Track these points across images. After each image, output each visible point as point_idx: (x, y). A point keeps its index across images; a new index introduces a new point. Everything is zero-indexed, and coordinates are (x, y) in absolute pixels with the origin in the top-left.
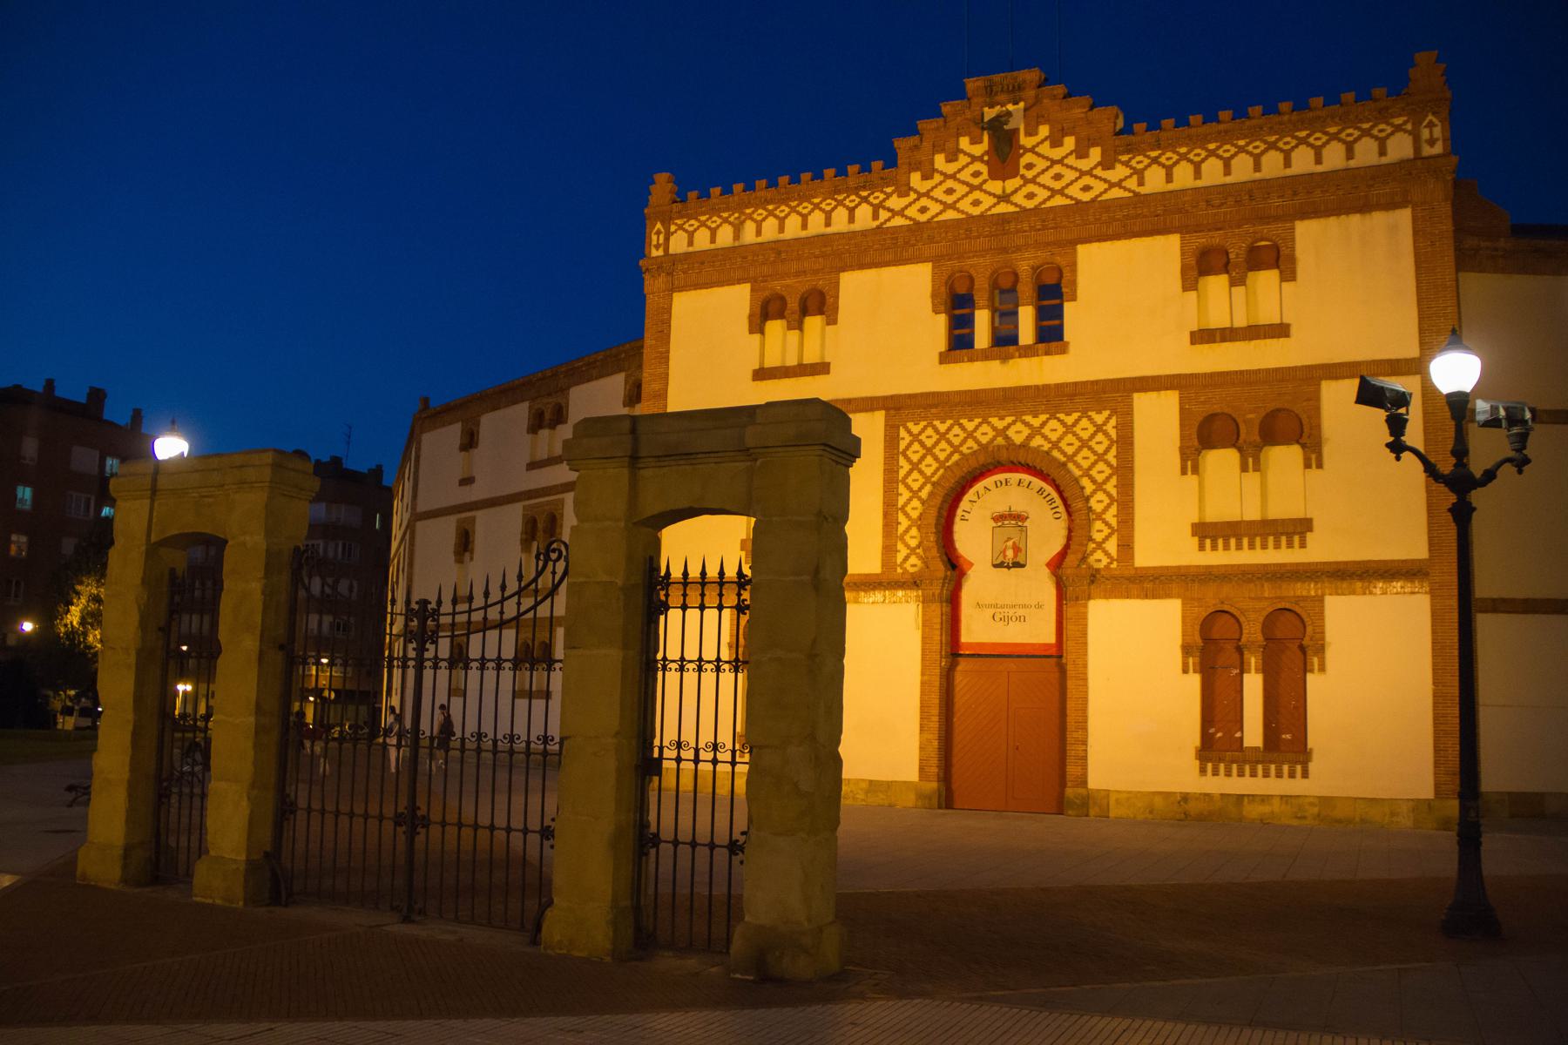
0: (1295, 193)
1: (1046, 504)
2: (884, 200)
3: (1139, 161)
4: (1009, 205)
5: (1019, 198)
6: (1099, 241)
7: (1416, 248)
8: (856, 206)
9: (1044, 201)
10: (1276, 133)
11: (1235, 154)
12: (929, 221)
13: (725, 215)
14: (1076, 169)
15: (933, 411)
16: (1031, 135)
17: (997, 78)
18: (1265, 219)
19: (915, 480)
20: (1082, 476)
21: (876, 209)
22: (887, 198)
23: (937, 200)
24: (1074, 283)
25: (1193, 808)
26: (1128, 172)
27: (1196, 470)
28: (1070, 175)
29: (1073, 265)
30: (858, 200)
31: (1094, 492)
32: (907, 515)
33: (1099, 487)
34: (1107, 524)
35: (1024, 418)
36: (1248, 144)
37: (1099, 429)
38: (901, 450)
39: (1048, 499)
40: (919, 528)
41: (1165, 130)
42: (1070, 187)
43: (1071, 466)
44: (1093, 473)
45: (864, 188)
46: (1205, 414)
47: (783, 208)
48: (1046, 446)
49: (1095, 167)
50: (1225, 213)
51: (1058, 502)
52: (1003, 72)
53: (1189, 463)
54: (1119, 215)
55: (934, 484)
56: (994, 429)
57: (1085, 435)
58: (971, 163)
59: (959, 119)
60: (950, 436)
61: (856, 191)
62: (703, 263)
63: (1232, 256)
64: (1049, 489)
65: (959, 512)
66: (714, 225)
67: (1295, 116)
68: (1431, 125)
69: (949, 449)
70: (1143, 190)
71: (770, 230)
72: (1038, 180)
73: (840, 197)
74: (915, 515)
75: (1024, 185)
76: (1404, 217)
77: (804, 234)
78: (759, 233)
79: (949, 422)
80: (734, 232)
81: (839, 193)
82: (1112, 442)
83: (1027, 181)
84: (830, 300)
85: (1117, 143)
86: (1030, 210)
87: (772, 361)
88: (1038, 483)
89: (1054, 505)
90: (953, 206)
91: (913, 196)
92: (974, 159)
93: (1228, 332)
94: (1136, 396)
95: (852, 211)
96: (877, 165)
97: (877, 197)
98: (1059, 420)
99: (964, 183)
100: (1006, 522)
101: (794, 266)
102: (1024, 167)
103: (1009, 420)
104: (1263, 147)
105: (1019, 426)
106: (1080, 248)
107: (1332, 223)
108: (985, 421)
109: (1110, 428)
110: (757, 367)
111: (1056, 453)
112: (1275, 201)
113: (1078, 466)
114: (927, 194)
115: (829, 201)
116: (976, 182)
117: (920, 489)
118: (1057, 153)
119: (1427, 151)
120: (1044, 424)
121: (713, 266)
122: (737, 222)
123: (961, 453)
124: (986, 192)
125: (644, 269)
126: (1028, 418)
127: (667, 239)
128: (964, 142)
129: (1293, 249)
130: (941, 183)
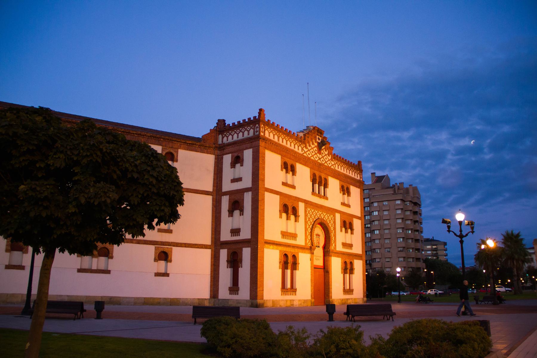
15: (312, 206)
21: (302, 149)
25: (343, 301)
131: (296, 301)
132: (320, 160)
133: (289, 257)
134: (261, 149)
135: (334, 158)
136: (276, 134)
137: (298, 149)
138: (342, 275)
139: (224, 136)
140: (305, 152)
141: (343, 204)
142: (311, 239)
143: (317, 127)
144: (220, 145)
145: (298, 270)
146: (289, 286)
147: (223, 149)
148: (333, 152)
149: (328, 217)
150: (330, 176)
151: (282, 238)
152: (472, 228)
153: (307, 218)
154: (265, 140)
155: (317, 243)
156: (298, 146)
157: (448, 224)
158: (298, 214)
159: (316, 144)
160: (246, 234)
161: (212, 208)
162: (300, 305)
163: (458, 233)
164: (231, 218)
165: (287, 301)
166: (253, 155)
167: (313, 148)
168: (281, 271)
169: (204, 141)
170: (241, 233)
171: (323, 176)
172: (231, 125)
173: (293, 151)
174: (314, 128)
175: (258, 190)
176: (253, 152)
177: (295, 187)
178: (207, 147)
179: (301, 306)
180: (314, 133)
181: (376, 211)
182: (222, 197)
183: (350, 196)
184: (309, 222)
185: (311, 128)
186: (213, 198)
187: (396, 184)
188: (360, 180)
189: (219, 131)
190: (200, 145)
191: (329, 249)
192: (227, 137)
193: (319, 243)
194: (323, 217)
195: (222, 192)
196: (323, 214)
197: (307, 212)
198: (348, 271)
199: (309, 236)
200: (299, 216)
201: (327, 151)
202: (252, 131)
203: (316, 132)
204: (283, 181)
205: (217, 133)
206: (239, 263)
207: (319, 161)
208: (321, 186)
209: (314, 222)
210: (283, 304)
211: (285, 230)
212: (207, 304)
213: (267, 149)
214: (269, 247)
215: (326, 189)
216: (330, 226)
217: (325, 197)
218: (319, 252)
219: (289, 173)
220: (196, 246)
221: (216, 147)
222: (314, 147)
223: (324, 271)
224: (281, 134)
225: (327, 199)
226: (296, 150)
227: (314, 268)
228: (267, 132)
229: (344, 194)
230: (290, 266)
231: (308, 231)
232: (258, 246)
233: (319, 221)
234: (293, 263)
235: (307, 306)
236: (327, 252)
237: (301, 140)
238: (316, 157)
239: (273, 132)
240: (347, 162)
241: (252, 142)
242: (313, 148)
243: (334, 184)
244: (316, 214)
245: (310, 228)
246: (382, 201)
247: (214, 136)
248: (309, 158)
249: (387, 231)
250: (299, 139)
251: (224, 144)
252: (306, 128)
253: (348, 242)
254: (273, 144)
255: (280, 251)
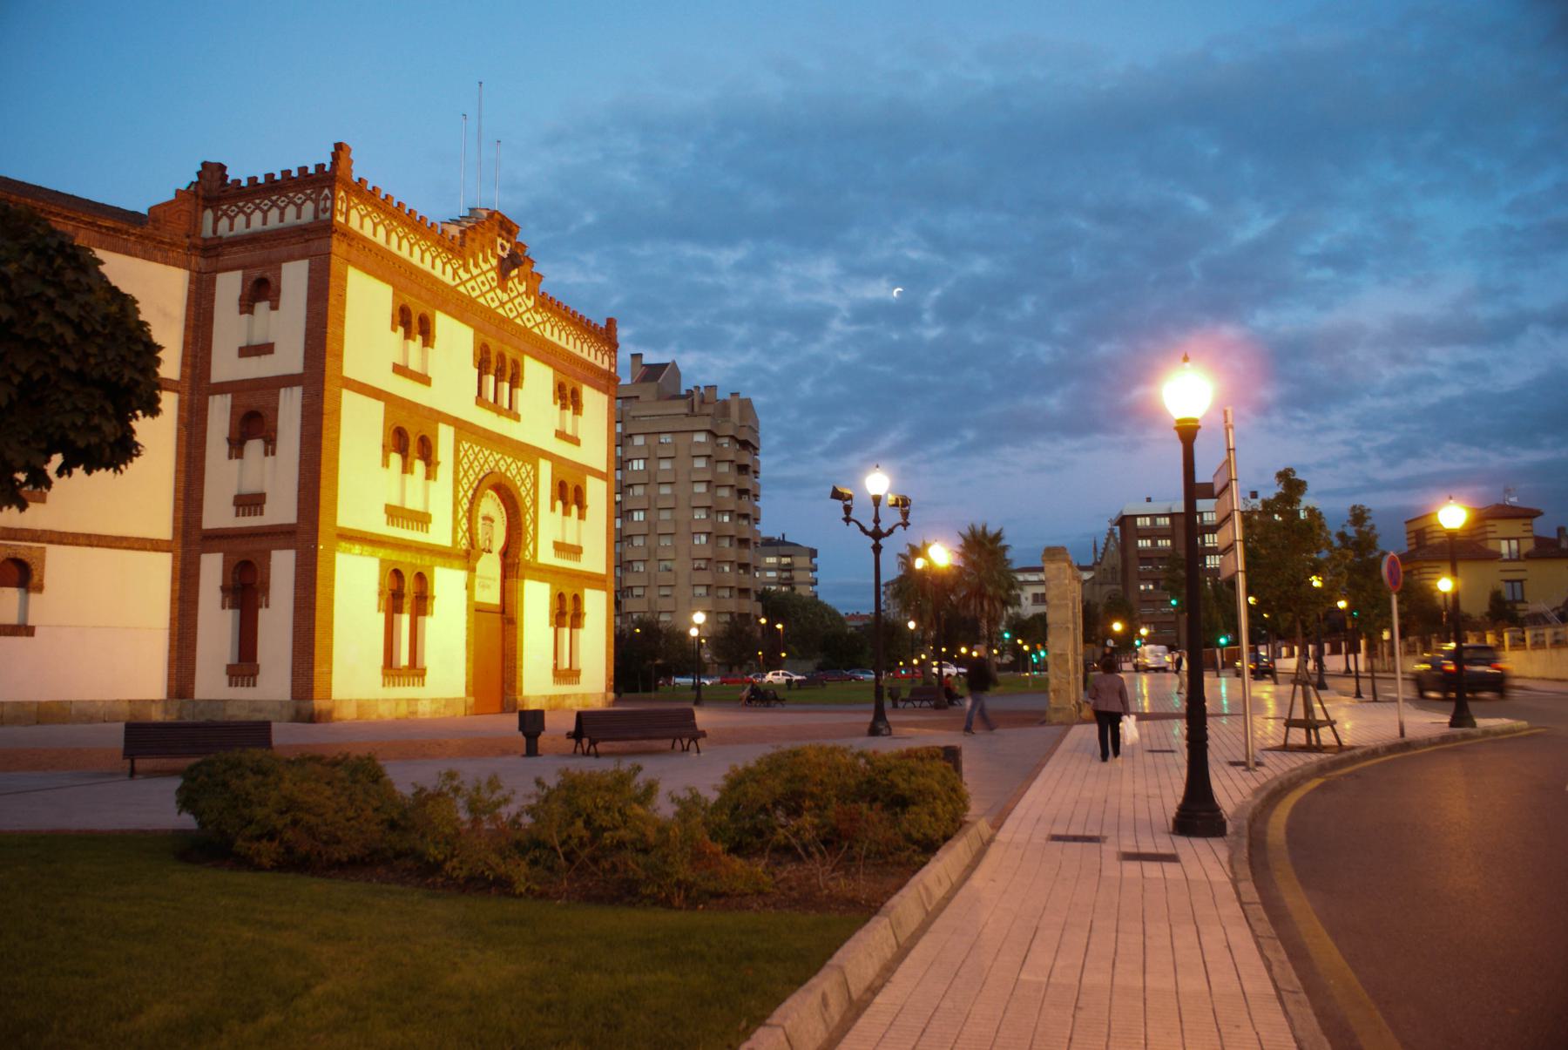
15: (474, 436)
21: (455, 273)
131: (424, 702)
132: (504, 308)
133: (406, 579)
134: (335, 262)
135: (543, 305)
136: (381, 222)
137: (442, 270)
138: (552, 630)
139: (222, 216)
140: (463, 283)
141: (561, 435)
142: (470, 529)
143: (499, 214)
144: (205, 240)
145: (432, 614)
146: (404, 660)
147: (218, 255)
148: (542, 288)
149: (519, 469)
150: (528, 354)
151: (388, 524)
152: (905, 515)
153: (461, 469)
154: (349, 236)
155: (485, 541)
156: (444, 264)
157: (846, 500)
158: (436, 457)
159: (494, 262)
160: (281, 510)
161: (179, 430)
162: (435, 712)
163: (870, 527)
164: (236, 462)
165: (397, 702)
166: (310, 278)
167: (484, 273)
168: (382, 616)
169: (157, 225)
170: (266, 507)
171: (509, 354)
172: (244, 183)
173: (427, 275)
174: (492, 214)
175: (323, 382)
176: (311, 270)
177: (430, 379)
178: (163, 243)
179: (437, 716)
180: (490, 230)
181: (638, 459)
182: (211, 398)
183: (581, 415)
184: (465, 480)
185: (482, 215)
186: (181, 402)
187: (697, 388)
188: (609, 371)
189: (204, 199)
190: (141, 236)
191: (519, 560)
192: (232, 219)
193: (490, 541)
194: (503, 470)
195: (209, 383)
196: (505, 461)
197: (461, 454)
198: (568, 619)
199: (464, 521)
200: (438, 463)
201: (524, 284)
202: (309, 208)
203: (497, 228)
204: (397, 362)
205: (198, 205)
206: (260, 595)
207: (500, 311)
208: (503, 380)
209: (480, 482)
210: (386, 712)
211: (395, 502)
212: (157, 716)
213: (352, 265)
214: (350, 549)
215: (514, 390)
216: (524, 494)
217: (512, 413)
218: (490, 566)
219: (414, 340)
220: (125, 544)
221: (193, 247)
222: (488, 271)
223: (503, 619)
224: (395, 224)
225: (517, 417)
226: (437, 272)
227: (476, 610)
228: (353, 213)
229: (564, 407)
230: (407, 603)
231: (462, 507)
232: (316, 546)
233: (492, 480)
234: (416, 597)
235: (455, 716)
236: (512, 566)
237: (452, 245)
238: (492, 299)
239: (372, 216)
240: (577, 320)
241: (307, 241)
242: (484, 273)
243: (538, 377)
244: (486, 461)
245: (467, 497)
246: (655, 433)
247: (190, 212)
248: (473, 301)
249: (665, 515)
250: (447, 244)
251: (220, 237)
252: (467, 213)
253: (571, 540)
254: (370, 251)
255: (382, 561)
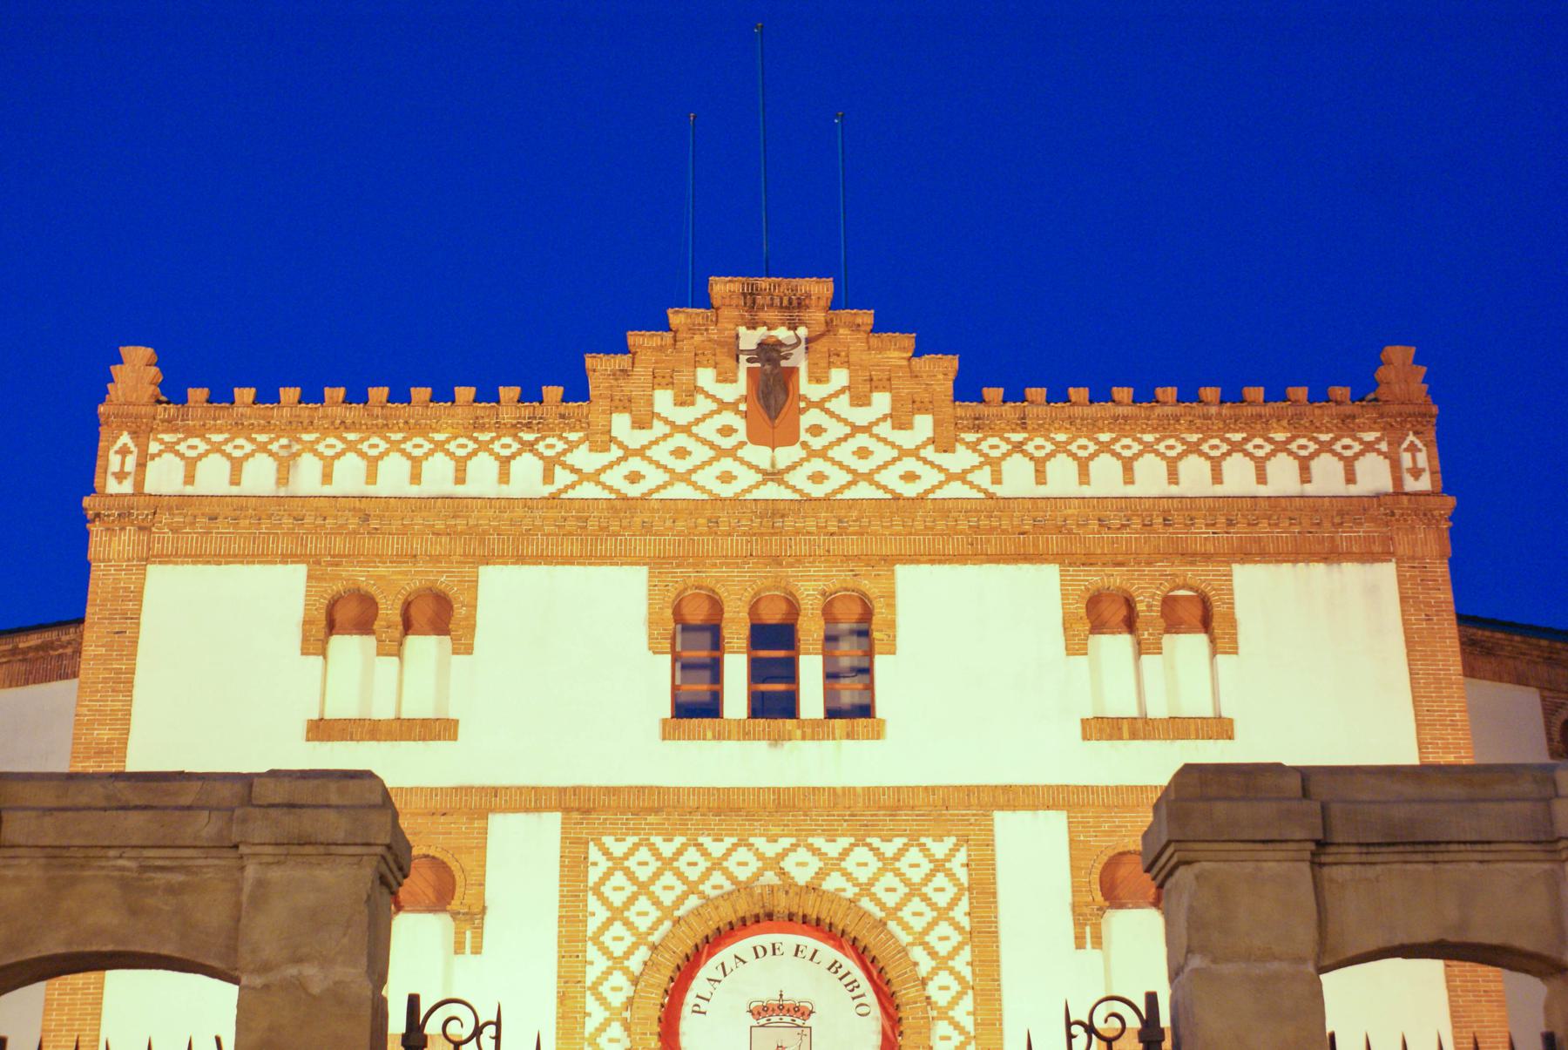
0: (1230, 523)
1: (845, 991)
2: (564, 452)
3: (994, 445)
4: (782, 487)
5: (798, 478)
6: (932, 562)
7: (1405, 622)
8: (513, 456)
9: (842, 488)
10: (1198, 430)
11: (1140, 454)
12: (644, 498)
13: (262, 438)
14: (893, 445)
15: (652, 819)
16: (819, 381)
17: (764, 283)
18: (1190, 557)
19: (618, 939)
20: (912, 944)
21: (550, 466)
22: (570, 450)
23: (658, 465)
24: (892, 625)
26: (975, 459)
27: (1098, 942)
28: (882, 453)
29: (890, 596)
30: (516, 446)
31: (935, 971)
32: (601, 999)
33: (942, 963)
34: (957, 1026)
35: (810, 840)
36: (1158, 441)
37: (939, 866)
38: (591, 884)
39: (847, 980)
40: (627, 1027)
41: (1074, 404)
42: (883, 471)
43: (892, 925)
44: (931, 938)
45: (529, 426)
46: (1111, 853)
47: (375, 440)
48: (851, 892)
49: (924, 445)
50: (1128, 540)
51: (865, 986)
52: (743, 276)
53: (1088, 929)
54: (963, 525)
55: (654, 948)
56: (760, 856)
57: (916, 876)
58: (719, 412)
59: (698, 338)
60: (681, 864)
61: (514, 429)
62: (213, 518)
63: (1141, 607)
64: (850, 965)
65: (690, 999)
66: (237, 453)
67: (1227, 409)
68: (1412, 448)
69: (680, 888)
70: (1000, 491)
71: (349, 477)
72: (830, 454)
73: (484, 437)
74: (617, 1000)
75: (807, 459)
76: (1386, 573)
77: (414, 491)
78: (327, 477)
79: (679, 841)
80: (278, 471)
81: (483, 428)
82: (961, 889)
83: (812, 454)
84: (460, 612)
85: (960, 412)
86: (819, 499)
87: (341, 707)
88: (828, 952)
89: (857, 992)
90: (686, 478)
91: (616, 452)
92: (723, 406)
93: (1140, 724)
94: (999, 816)
95: (505, 462)
96: (553, 393)
97: (552, 446)
98: (869, 845)
99: (704, 442)
100: (774, 1019)
101: (393, 545)
102: (807, 430)
103: (785, 842)
104: (1180, 448)
105: (802, 854)
106: (900, 569)
107: (1286, 573)
108: (743, 842)
109: (957, 864)
110: (316, 717)
111: (866, 904)
112: (1201, 530)
113: (906, 927)
114: (641, 452)
115: (461, 441)
116: (727, 443)
117: (628, 954)
118: (861, 416)
119: (1411, 485)
120: (845, 853)
121: (236, 526)
122: (283, 453)
123: (702, 894)
124: (742, 461)
125: (90, 513)
126: (818, 842)
127: (141, 466)
128: (706, 377)
129: (1231, 604)
130: (665, 437)
183: (1234, 650)
